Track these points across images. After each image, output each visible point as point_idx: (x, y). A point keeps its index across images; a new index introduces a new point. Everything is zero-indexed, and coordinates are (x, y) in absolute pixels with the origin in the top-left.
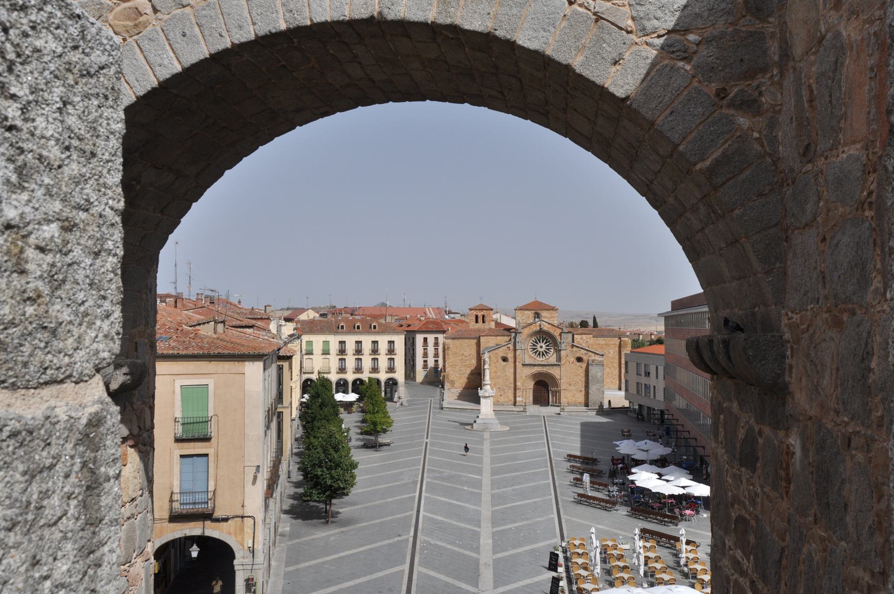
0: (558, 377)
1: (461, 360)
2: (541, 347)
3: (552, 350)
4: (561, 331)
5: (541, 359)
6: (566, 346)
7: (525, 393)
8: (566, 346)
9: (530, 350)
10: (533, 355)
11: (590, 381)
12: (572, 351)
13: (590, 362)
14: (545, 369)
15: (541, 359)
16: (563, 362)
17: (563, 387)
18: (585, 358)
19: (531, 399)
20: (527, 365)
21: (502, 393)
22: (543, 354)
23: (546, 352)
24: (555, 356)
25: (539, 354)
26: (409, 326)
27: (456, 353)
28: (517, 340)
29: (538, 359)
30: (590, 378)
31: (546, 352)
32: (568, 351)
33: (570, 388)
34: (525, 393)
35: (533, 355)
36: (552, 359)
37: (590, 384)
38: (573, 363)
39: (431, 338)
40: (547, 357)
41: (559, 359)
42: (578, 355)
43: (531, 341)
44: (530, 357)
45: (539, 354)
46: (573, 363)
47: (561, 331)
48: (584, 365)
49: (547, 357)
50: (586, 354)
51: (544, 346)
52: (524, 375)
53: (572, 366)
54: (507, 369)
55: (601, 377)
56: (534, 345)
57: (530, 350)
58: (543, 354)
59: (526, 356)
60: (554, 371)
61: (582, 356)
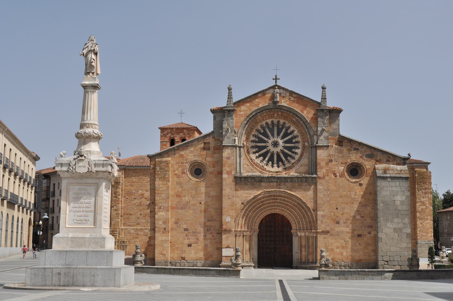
0: (310, 205)
1: (140, 205)
2: (275, 144)
3: (299, 151)
8: (327, 138)
11: (380, 214)
13: (379, 173)
15: (276, 169)
16: (320, 173)
21: (192, 239)
22: (279, 159)
23: (286, 155)
24: (305, 161)
25: (271, 159)
27: (129, 193)
28: (225, 126)
29: (269, 168)
30: (380, 206)
31: (286, 155)
32: (332, 151)
33: (339, 228)
35: (258, 161)
37: (381, 220)
38: (342, 175)
40: (288, 165)
46: (342, 175)
48: (365, 180)
49: (288, 165)
51: (281, 142)
53: (339, 179)
58: (279, 159)
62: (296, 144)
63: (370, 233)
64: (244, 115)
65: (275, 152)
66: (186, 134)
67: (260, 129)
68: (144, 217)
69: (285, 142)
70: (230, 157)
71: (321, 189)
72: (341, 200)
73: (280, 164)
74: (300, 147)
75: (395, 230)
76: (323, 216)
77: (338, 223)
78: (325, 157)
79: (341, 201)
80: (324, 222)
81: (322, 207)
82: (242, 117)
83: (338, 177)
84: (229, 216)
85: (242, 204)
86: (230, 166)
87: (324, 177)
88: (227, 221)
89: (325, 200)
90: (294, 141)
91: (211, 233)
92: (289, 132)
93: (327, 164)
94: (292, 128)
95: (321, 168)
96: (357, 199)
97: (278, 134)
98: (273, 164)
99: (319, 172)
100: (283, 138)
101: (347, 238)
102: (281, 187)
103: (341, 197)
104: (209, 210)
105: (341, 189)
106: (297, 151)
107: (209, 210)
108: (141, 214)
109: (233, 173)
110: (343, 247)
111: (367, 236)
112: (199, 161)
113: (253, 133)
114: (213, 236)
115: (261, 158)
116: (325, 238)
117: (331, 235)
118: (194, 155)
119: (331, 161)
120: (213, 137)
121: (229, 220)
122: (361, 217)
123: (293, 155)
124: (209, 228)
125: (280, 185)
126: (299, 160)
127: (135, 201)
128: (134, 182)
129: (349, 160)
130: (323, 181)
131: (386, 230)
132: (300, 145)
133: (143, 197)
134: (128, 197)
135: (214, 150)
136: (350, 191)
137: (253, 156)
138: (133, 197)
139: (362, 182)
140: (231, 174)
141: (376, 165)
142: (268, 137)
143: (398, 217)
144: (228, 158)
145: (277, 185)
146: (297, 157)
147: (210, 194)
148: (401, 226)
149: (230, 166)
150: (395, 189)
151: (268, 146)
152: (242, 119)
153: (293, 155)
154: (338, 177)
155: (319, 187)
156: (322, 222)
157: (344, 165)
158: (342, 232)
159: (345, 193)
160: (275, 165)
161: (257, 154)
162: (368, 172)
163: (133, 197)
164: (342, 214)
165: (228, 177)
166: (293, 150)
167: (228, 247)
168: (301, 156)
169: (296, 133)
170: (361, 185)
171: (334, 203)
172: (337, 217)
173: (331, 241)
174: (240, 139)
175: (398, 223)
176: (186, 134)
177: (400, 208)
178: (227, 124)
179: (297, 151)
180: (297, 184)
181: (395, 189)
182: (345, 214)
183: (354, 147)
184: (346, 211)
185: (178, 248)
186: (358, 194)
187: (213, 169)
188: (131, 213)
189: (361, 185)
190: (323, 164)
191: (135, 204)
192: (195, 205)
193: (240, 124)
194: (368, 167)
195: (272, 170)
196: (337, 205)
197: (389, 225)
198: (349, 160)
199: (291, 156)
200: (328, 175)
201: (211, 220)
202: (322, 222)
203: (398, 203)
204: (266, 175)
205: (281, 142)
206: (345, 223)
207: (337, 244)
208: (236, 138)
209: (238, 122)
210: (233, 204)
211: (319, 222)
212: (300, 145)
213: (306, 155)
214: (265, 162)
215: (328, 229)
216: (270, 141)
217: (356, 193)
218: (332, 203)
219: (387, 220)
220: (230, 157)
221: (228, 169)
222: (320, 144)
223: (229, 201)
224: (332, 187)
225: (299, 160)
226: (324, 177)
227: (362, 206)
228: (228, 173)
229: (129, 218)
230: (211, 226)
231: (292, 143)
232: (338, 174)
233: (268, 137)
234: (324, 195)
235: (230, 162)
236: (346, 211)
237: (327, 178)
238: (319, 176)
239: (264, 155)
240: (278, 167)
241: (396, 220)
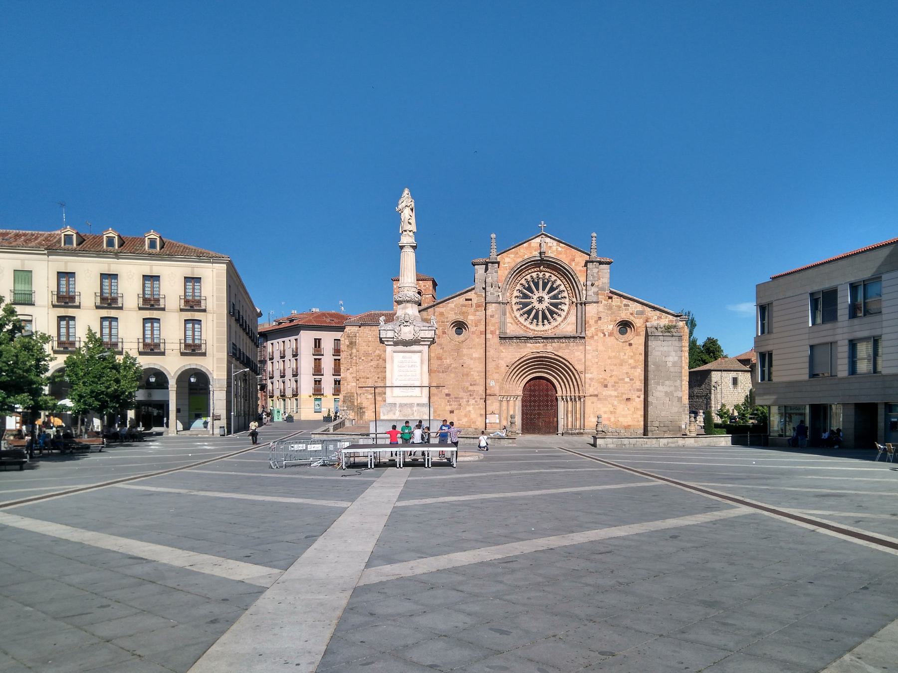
0: (580, 367)
3: (565, 308)
4: (587, 258)
5: (540, 328)
6: (597, 294)
7: (504, 403)
9: (515, 307)
10: (522, 320)
12: (610, 308)
14: (550, 349)
15: (540, 328)
16: (589, 333)
17: (590, 390)
18: (638, 322)
19: (518, 420)
20: (511, 338)
24: (572, 318)
25: (536, 317)
26: (291, 321)
29: (533, 327)
32: (601, 307)
34: (504, 403)
35: (522, 320)
36: (566, 324)
38: (611, 334)
39: (328, 339)
41: (582, 323)
42: (624, 316)
43: (519, 287)
44: (518, 323)
45: (536, 317)
46: (611, 334)
47: (587, 258)
50: (641, 313)
51: (546, 297)
52: (503, 364)
54: (465, 351)
55: (674, 364)
56: (525, 296)
57: (515, 307)
58: (544, 317)
59: (509, 320)
60: (572, 354)
61: (631, 319)
62: (563, 300)
63: (639, 397)
64: (508, 268)
65: (540, 309)
66: (422, 286)
67: (524, 283)
68: (382, 380)
69: (551, 298)
70: (494, 315)
71: (589, 350)
72: (609, 361)
73: (546, 321)
74: (567, 303)
75: (666, 393)
76: (591, 379)
77: (606, 386)
78: (595, 314)
79: (609, 362)
80: (592, 386)
81: (590, 370)
82: (507, 270)
83: (607, 336)
84: (494, 380)
85: (507, 366)
86: (493, 325)
87: (592, 337)
88: (491, 385)
89: (593, 361)
90: (560, 296)
91: (474, 399)
92: (554, 286)
93: (596, 322)
94: (559, 282)
95: (590, 326)
96: (625, 360)
97: (544, 289)
98: (537, 322)
99: (588, 331)
100: (549, 293)
101: (616, 402)
102: (547, 347)
103: (610, 358)
104: (472, 373)
105: (610, 350)
106: (563, 307)
107: (472, 373)
108: (378, 378)
109: (497, 333)
110: (611, 412)
111: (636, 401)
112: (460, 320)
113: (517, 288)
114: (476, 402)
115: (526, 315)
116: (593, 403)
117: (599, 400)
118: (455, 313)
119: (600, 318)
120: (476, 293)
121: (494, 384)
122: (630, 380)
123: (559, 312)
124: (471, 393)
125: (546, 345)
126: (565, 318)
127: (372, 364)
128: (370, 342)
129: (619, 318)
130: (592, 342)
131: (657, 394)
132: (567, 301)
133: (380, 358)
134: (363, 358)
135: (476, 307)
136: (619, 352)
137: (518, 314)
138: (370, 358)
139: (632, 342)
140: (495, 333)
141: (647, 323)
142: (532, 292)
143: (669, 379)
144: (492, 316)
145: (543, 346)
146: (563, 316)
147: (472, 356)
148: (672, 388)
149: (493, 325)
150: (665, 349)
151: (532, 303)
152: (507, 272)
153: (559, 312)
154: (607, 336)
155: (588, 348)
156: (590, 386)
157: (613, 323)
158: (611, 396)
159: (614, 354)
160: (540, 323)
161: (521, 312)
162: (638, 331)
163: (370, 358)
164: (611, 377)
165: (492, 338)
166: (560, 306)
167: (493, 413)
168: (568, 313)
169: (562, 288)
170: (630, 345)
171: (602, 365)
172: (605, 379)
173: (599, 406)
174: (503, 294)
175: (670, 386)
176: (422, 286)
177: (672, 369)
178: (490, 278)
179: (563, 307)
180: (564, 344)
181: (665, 349)
182: (613, 377)
183: (624, 303)
184: (614, 373)
185: (439, 414)
186: (627, 355)
187: (476, 328)
188: (368, 376)
189: (630, 345)
190: (592, 322)
191: (372, 366)
192: (456, 369)
193: (504, 279)
194: (638, 325)
195: (537, 329)
196: (605, 367)
197: (660, 388)
198: (619, 318)
199: (556, 313)
200: (597, 335)
201: (475, 385)
202: (590, 386)
203: (670, 364)
204: (531, 334)
205: (546, 297)
206: (613, 386)
207: (605, 409)
208: (500, 294)
209: (502, 275)
210: (497, 367)
211: (587, 386)
212: (567, 301)
213: (573, 311)
214: (529, 320)
215: (596, 393)
216: (535, 297)
217: (625, 354)
218: (600, 365)
219: (658, 384)
220: (494, 315)
221: (492, 328)
222: (589, 299)
223: (494, 363)
224: (601, 348)
225: (565, 318)
226: (592, 337)
227: (631, 368)
228: (492, 333)
229: (366, 382)
230: (474, 390)
231: (558, 299)
232: (607, 333)
233: (532, 292)
234: (592, 356)
235: (494, 320)
236: (614, 373)
237: (596, 338)
238: (588, 335)
239: (529, 313)
240: (543, 325)
241: (667, 382)
